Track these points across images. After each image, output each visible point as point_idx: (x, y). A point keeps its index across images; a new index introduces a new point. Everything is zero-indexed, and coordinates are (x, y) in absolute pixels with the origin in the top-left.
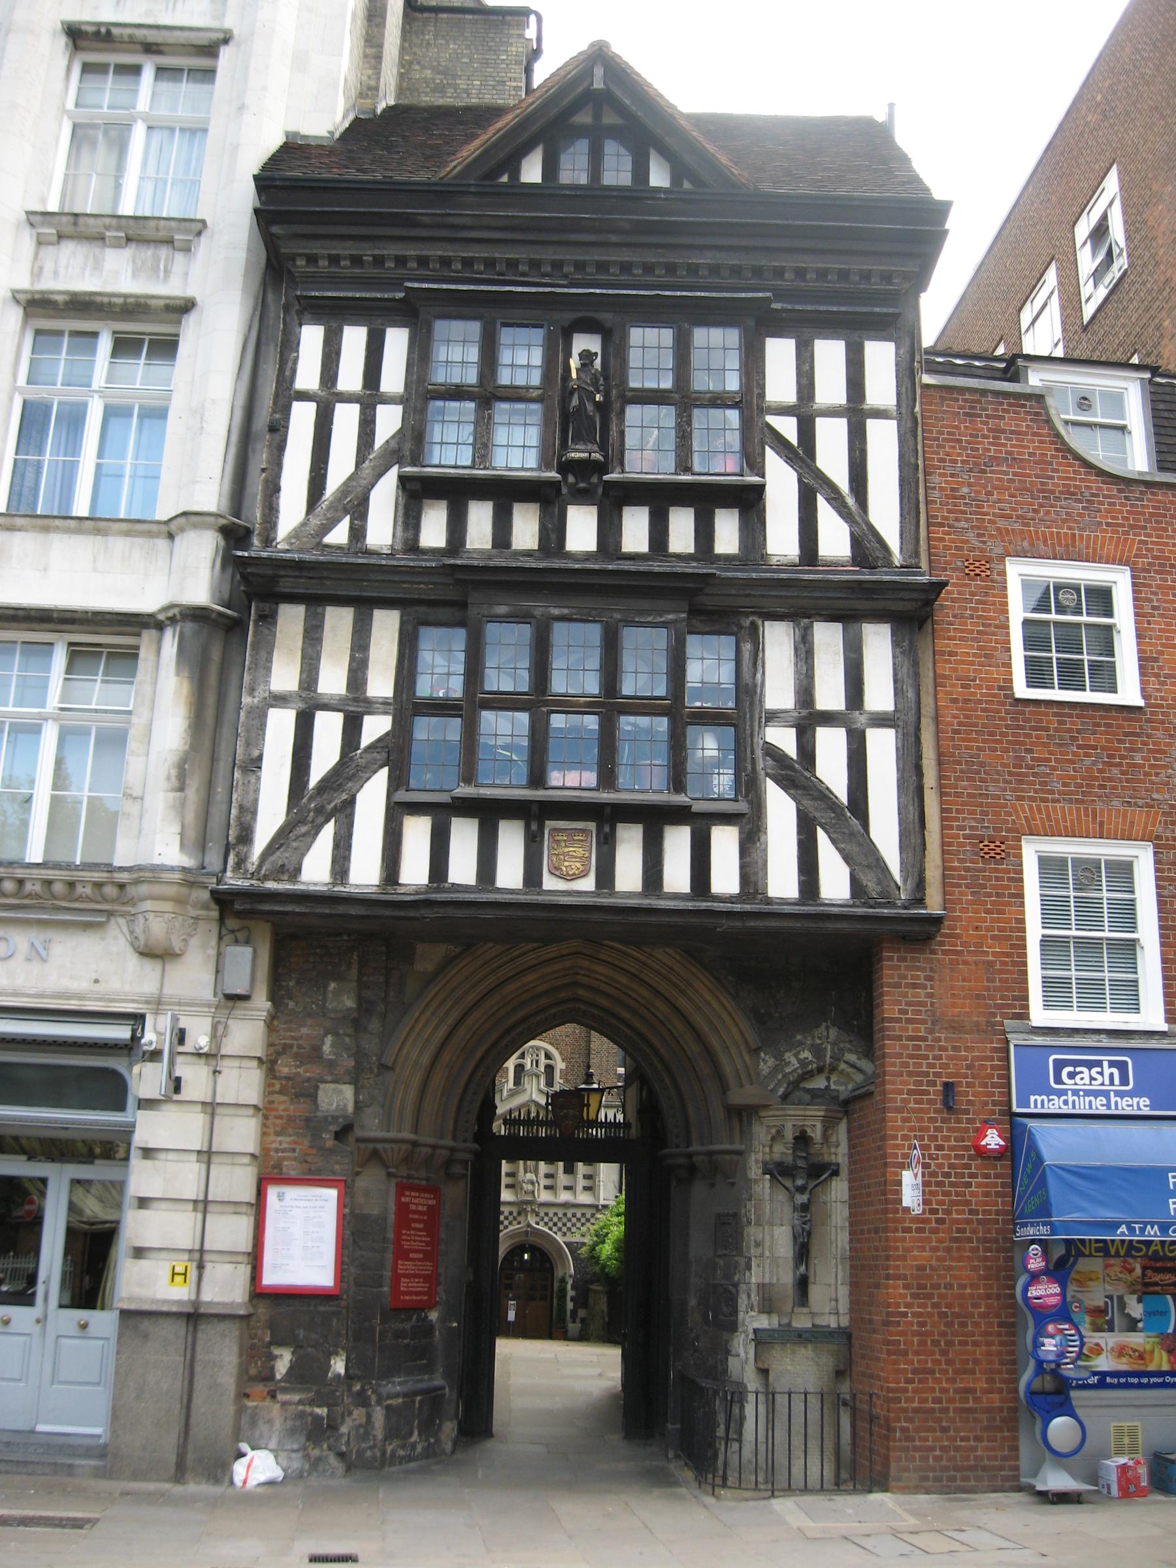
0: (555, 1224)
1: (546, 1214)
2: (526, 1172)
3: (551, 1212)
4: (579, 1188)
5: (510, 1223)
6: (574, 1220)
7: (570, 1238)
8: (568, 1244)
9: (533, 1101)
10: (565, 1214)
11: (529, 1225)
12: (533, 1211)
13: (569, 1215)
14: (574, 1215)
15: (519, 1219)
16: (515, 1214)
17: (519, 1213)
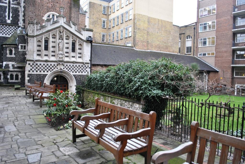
0: (70, 69)
1: (67, 65)
2: (59, 51)
3: (68, 64)
5: (54, 68)
6: (76, 67)
7: (74, 73)
8: (74, 75)
9: (62, 26)
10: (73, 66)
11: (61, 69)
12: (62, 64)
13: (75, 66)
14: (76, 66)
15: (57, 67)
16: (56, 65)
17: (57, 65)
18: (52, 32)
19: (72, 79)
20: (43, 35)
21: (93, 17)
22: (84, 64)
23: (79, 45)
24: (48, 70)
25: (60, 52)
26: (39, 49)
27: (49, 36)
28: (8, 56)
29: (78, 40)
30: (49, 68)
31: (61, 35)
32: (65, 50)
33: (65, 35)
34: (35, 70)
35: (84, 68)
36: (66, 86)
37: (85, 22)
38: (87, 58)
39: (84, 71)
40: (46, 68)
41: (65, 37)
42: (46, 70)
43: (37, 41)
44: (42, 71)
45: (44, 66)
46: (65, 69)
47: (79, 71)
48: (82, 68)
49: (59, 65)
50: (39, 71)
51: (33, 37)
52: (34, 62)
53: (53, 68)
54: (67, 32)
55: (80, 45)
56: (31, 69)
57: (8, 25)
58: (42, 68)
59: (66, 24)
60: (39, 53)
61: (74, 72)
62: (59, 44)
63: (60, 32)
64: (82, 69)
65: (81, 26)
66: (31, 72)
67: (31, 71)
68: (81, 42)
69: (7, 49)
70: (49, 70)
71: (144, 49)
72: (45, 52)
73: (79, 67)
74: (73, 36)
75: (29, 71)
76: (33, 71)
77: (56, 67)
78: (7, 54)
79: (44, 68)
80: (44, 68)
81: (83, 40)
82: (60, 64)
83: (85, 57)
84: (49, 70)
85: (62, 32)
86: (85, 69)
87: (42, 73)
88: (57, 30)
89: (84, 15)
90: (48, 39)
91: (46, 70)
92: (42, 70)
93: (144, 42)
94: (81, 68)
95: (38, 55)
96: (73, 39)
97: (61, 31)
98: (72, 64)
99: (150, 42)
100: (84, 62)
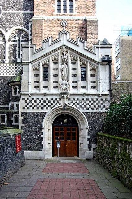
0: (78, 104)
1: (74, 99)
2: (63, 80)
3: (76, 98)
4: (89, 87)
5: (56, 104)
6: (88, 102)
7: (85, 111)
8: (85, 113)
9: (65, 45)
10: (83, 99)
11: (65, 104)
12: (67, 98)
13: (85, 99)
14: (88, 99)
15: (60, 102)
16: (58, 100)
17: (60, 99)
18: (52, 55)
19: (82, 119)
20: (40, 61)
22: (100, 97)
23: (91, 70)
24: (47, 106)
25: (64, 81)
26: (37, 79)
27: (48, 61)
28: (13, 95)
29: (89, 62)
30: (49, 104)
31: (64, 58)
32: (71, 79)
33: (70, 58)
34: (31, 106)
35: (99, 102)
36: (75, 129)
38: (104, 88)
39: (100, 106)
40: (45, 104)
41: (70, 61)
42: (45, 106)
43: (33, 70)
44: (40, 108)
45: (42, 102)
46: (72, 104)
47: (92, 106)
48: (97, 102)
49: (62, 99)
50: (35, 108)
51: (27, 64)
52: (30, 96)
53: (54, 104)
54: (72, 54)
55: (93, 69)
56: (26, 106)
57: (18, 64)
58: (40, 104)
59: (70, 42)
60: (36, 85)
61: (85, 108)
62: (62, 71)
63: (63, 55)
64: (97, 104)
66: (26, 110)
67: (26, 108)
68: (94, 65)
69: (12, 87)
70: (49, 106)
72: (42, 83)
73: (92, 102)
74: (81, 57)
75: (24, 108)
76: (28, 108)
77: (58, 102)
78: (12, 94)
79: (42, 104)
80: (42, 104)
81: (96, 61)
82: (64, 97)
83: (101, 86)
84: (49, 106)
85: (66, 55)
86: (102, 104)
87: (40, 110)
88: (59, 53)
90: (48, 65)
91: (45, 106)
92: (40, 106)
94: (94, 102)
95: (35, 87)
96: (81, 63)
97: (65, 53)
98: (81, 98)
100: (99, 93)
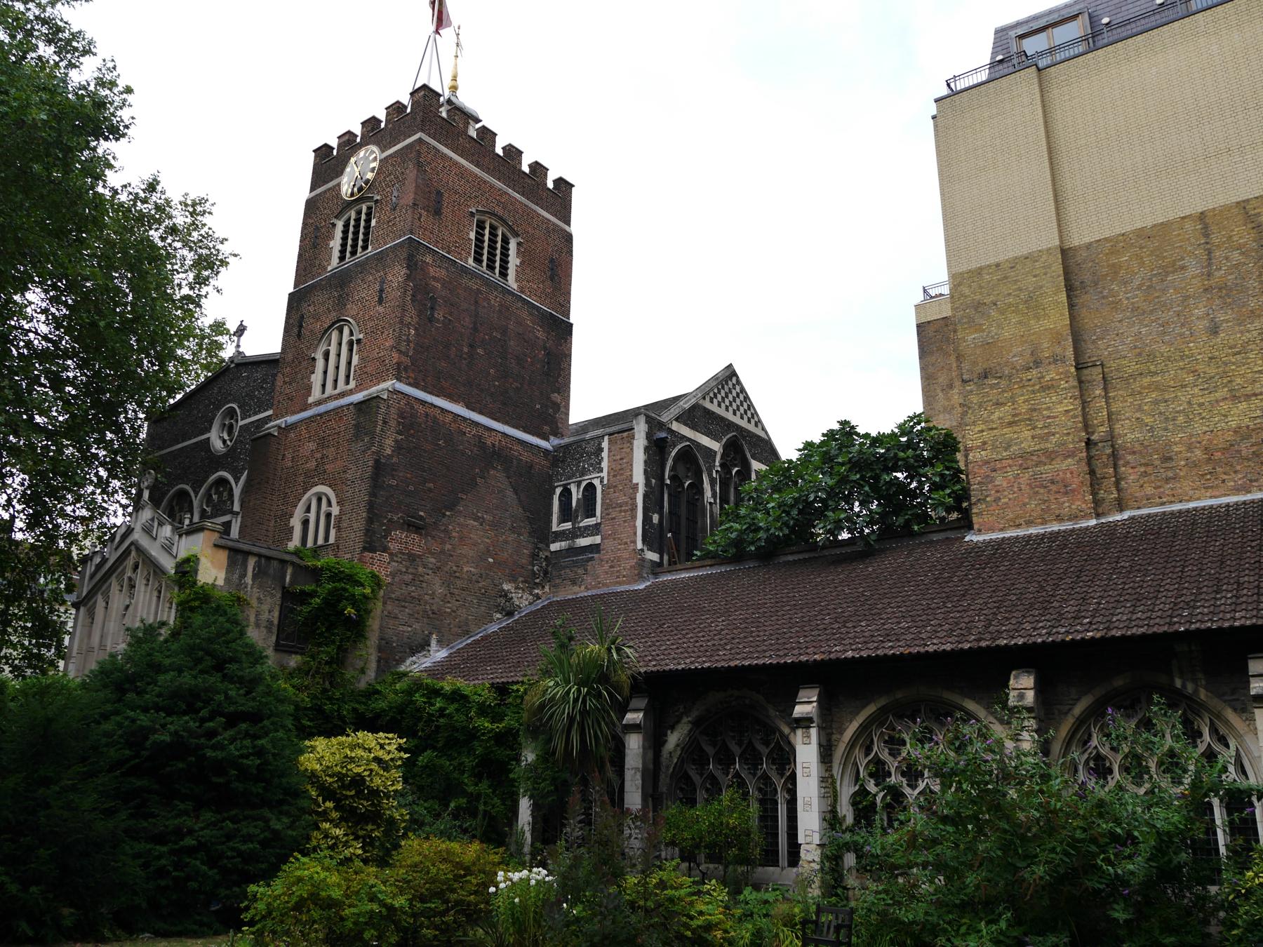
21: (949, 399)
37: (631, 470)
65: (612, 496)
71: (1059, 519)
89: (625, 434)
93: (1051, 456)
99: (1128, 434)
